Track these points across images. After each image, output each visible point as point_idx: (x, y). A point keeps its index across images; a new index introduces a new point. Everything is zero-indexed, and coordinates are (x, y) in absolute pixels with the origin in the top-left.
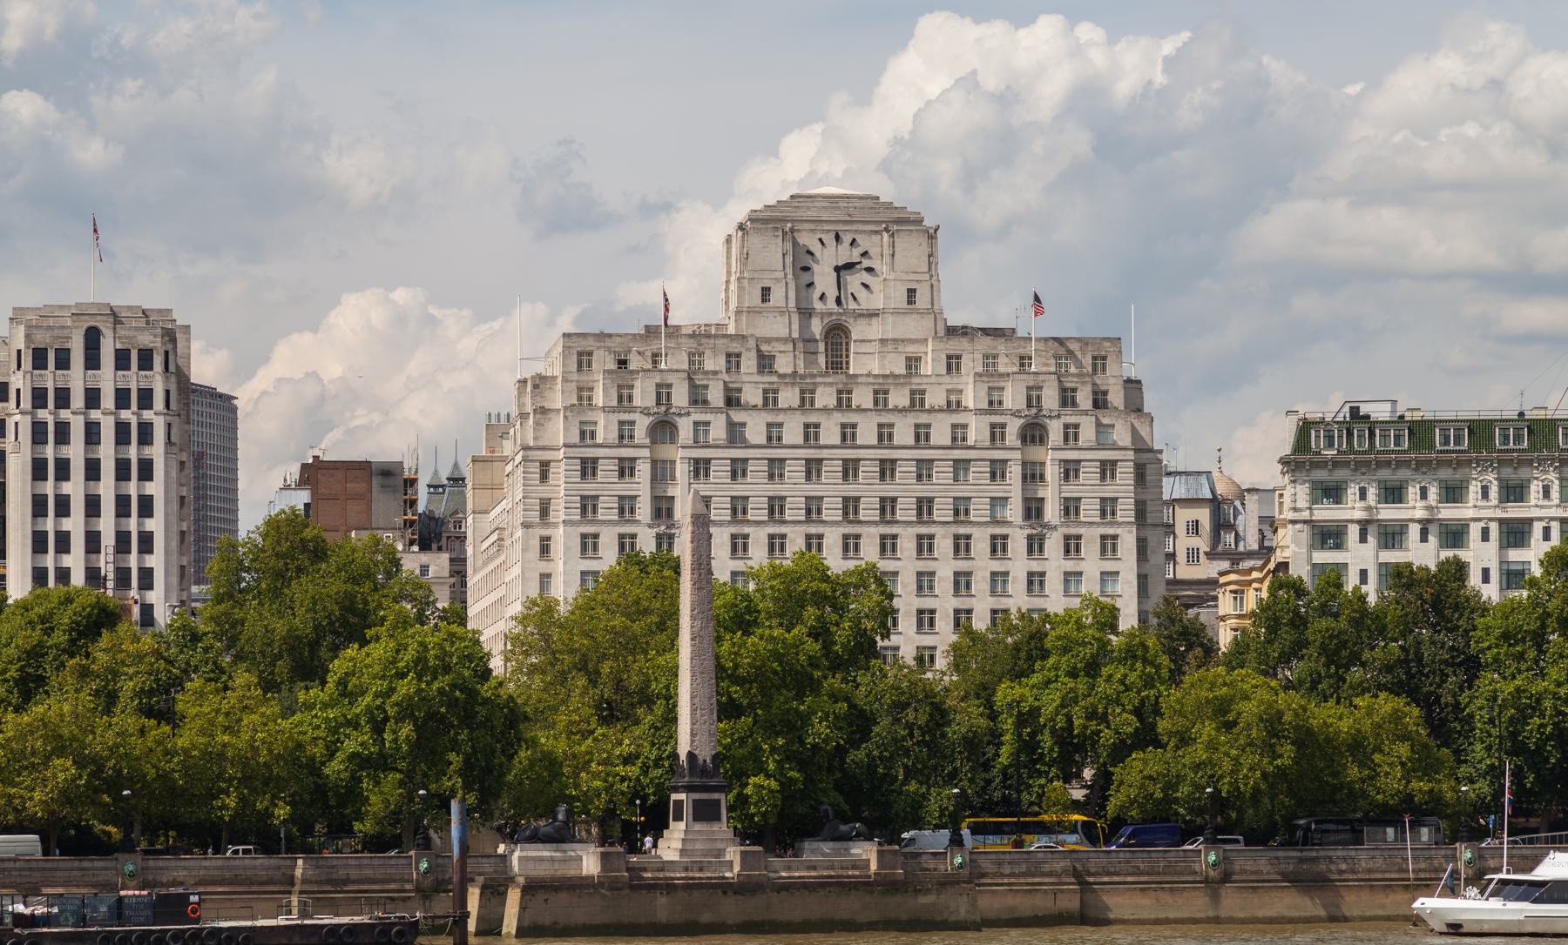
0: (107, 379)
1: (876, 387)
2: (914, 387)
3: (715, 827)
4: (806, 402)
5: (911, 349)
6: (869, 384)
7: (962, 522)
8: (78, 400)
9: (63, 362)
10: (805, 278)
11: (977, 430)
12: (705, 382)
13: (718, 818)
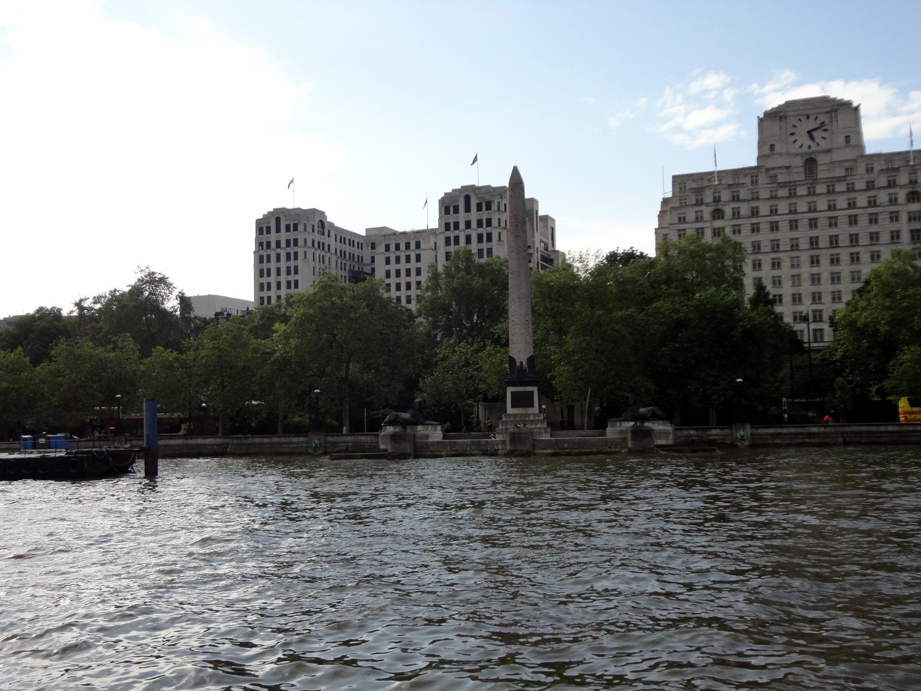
0: (474, 216)
1: (829, 184)
2: (848, 182)
3: (530, 411)
4: (792, 195)
5: (848, 164)
6: (824, 182)
7: (875, 244)
8: (462, 226)
9: (456, 211)
10: (793, 138)
11: (883, 197)
12: (738, 189)
13: (532, 406)
